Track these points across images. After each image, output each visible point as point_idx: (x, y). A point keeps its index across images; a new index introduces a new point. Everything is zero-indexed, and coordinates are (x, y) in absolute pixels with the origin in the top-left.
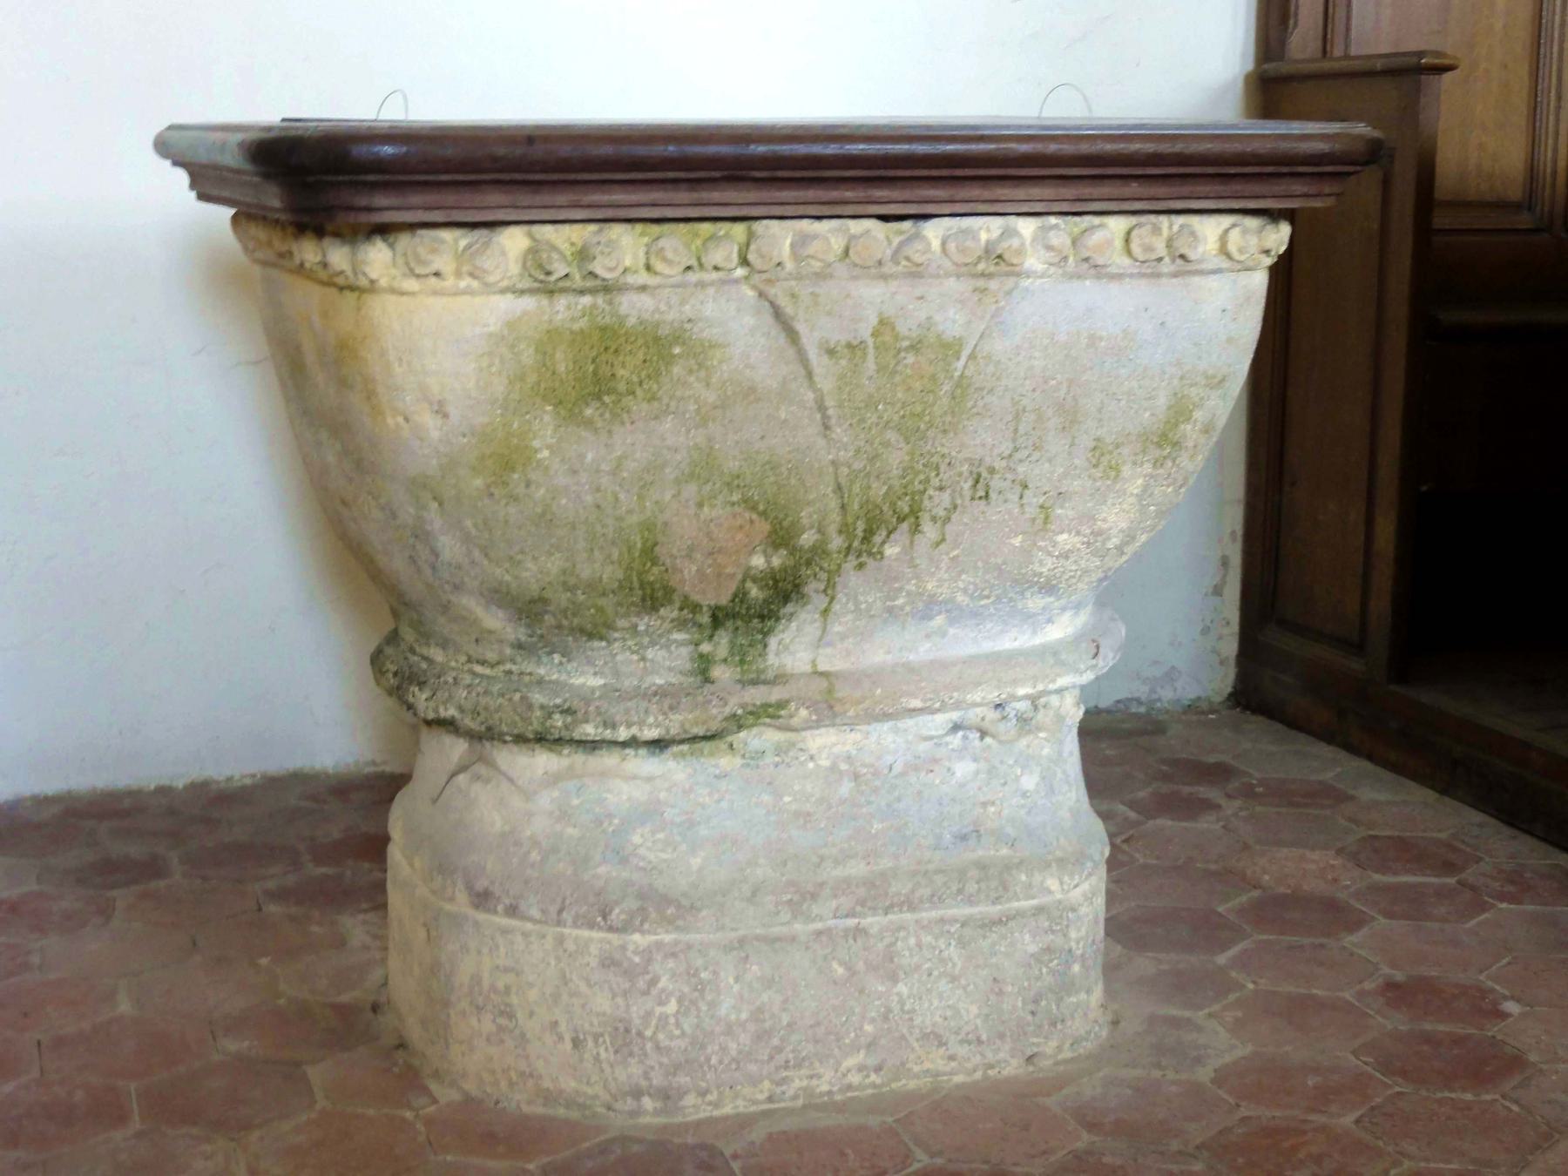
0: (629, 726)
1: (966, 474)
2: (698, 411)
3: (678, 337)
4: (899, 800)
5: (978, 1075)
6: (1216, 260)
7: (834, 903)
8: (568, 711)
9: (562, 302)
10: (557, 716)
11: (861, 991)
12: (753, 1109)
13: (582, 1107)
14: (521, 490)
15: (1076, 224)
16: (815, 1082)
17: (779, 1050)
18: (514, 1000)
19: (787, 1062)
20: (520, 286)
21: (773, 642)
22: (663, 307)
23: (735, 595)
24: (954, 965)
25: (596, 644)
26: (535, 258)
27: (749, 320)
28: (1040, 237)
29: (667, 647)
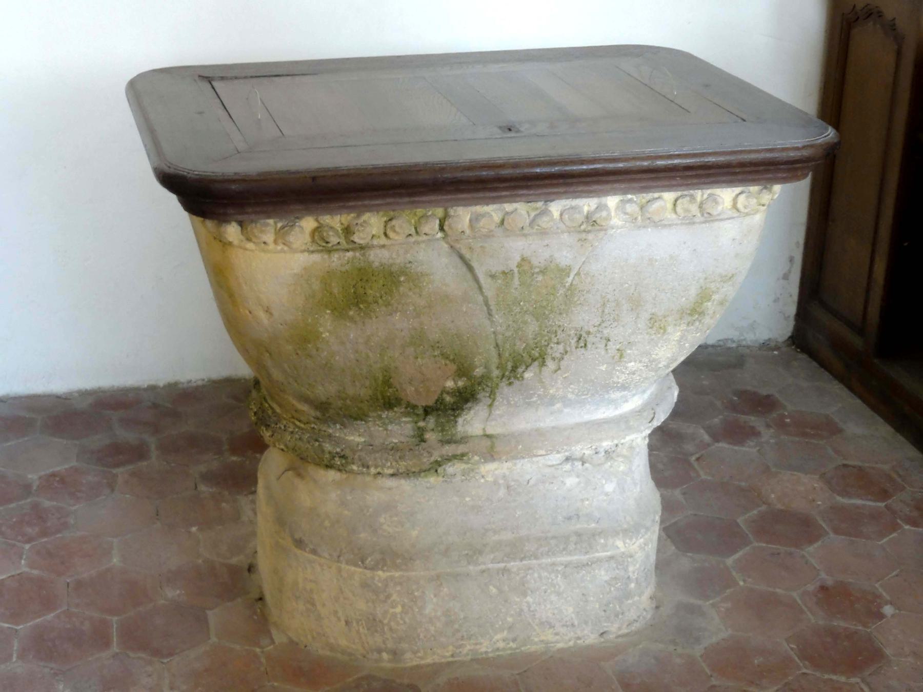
0: (376, 467)
1: (573, 335)
2: (415, 310)
3: (403, 272)
4: (532, 499)
5: (571, 643)
6: (730, 212)
7: (492, 556)
8: (343, 457)
9: (335, 256)
10: (337, 459)
11: (506, 601)
12: (443, 660)
13: (350, 654)
14: (314, 352)
15: (643, 198)
16: (478, 647)
17: (458, 631)
18: (315, 597)
19: (463, 637)
20: (311, 249)
21: (460, 420)
22: (394, 256)
23: (437, 401)
24: (560, 587)
25: (359, 422)
26: (318, 233)
27: (445, 260)
28: (621, 207)
29: (399, 424)
